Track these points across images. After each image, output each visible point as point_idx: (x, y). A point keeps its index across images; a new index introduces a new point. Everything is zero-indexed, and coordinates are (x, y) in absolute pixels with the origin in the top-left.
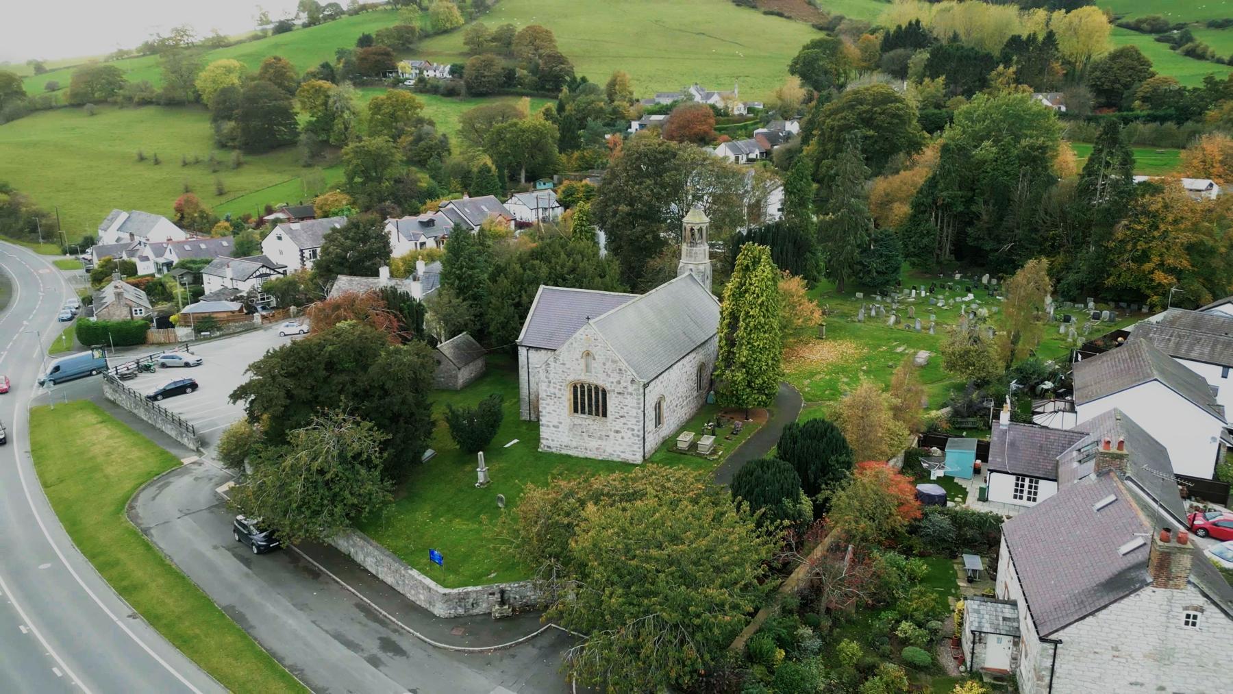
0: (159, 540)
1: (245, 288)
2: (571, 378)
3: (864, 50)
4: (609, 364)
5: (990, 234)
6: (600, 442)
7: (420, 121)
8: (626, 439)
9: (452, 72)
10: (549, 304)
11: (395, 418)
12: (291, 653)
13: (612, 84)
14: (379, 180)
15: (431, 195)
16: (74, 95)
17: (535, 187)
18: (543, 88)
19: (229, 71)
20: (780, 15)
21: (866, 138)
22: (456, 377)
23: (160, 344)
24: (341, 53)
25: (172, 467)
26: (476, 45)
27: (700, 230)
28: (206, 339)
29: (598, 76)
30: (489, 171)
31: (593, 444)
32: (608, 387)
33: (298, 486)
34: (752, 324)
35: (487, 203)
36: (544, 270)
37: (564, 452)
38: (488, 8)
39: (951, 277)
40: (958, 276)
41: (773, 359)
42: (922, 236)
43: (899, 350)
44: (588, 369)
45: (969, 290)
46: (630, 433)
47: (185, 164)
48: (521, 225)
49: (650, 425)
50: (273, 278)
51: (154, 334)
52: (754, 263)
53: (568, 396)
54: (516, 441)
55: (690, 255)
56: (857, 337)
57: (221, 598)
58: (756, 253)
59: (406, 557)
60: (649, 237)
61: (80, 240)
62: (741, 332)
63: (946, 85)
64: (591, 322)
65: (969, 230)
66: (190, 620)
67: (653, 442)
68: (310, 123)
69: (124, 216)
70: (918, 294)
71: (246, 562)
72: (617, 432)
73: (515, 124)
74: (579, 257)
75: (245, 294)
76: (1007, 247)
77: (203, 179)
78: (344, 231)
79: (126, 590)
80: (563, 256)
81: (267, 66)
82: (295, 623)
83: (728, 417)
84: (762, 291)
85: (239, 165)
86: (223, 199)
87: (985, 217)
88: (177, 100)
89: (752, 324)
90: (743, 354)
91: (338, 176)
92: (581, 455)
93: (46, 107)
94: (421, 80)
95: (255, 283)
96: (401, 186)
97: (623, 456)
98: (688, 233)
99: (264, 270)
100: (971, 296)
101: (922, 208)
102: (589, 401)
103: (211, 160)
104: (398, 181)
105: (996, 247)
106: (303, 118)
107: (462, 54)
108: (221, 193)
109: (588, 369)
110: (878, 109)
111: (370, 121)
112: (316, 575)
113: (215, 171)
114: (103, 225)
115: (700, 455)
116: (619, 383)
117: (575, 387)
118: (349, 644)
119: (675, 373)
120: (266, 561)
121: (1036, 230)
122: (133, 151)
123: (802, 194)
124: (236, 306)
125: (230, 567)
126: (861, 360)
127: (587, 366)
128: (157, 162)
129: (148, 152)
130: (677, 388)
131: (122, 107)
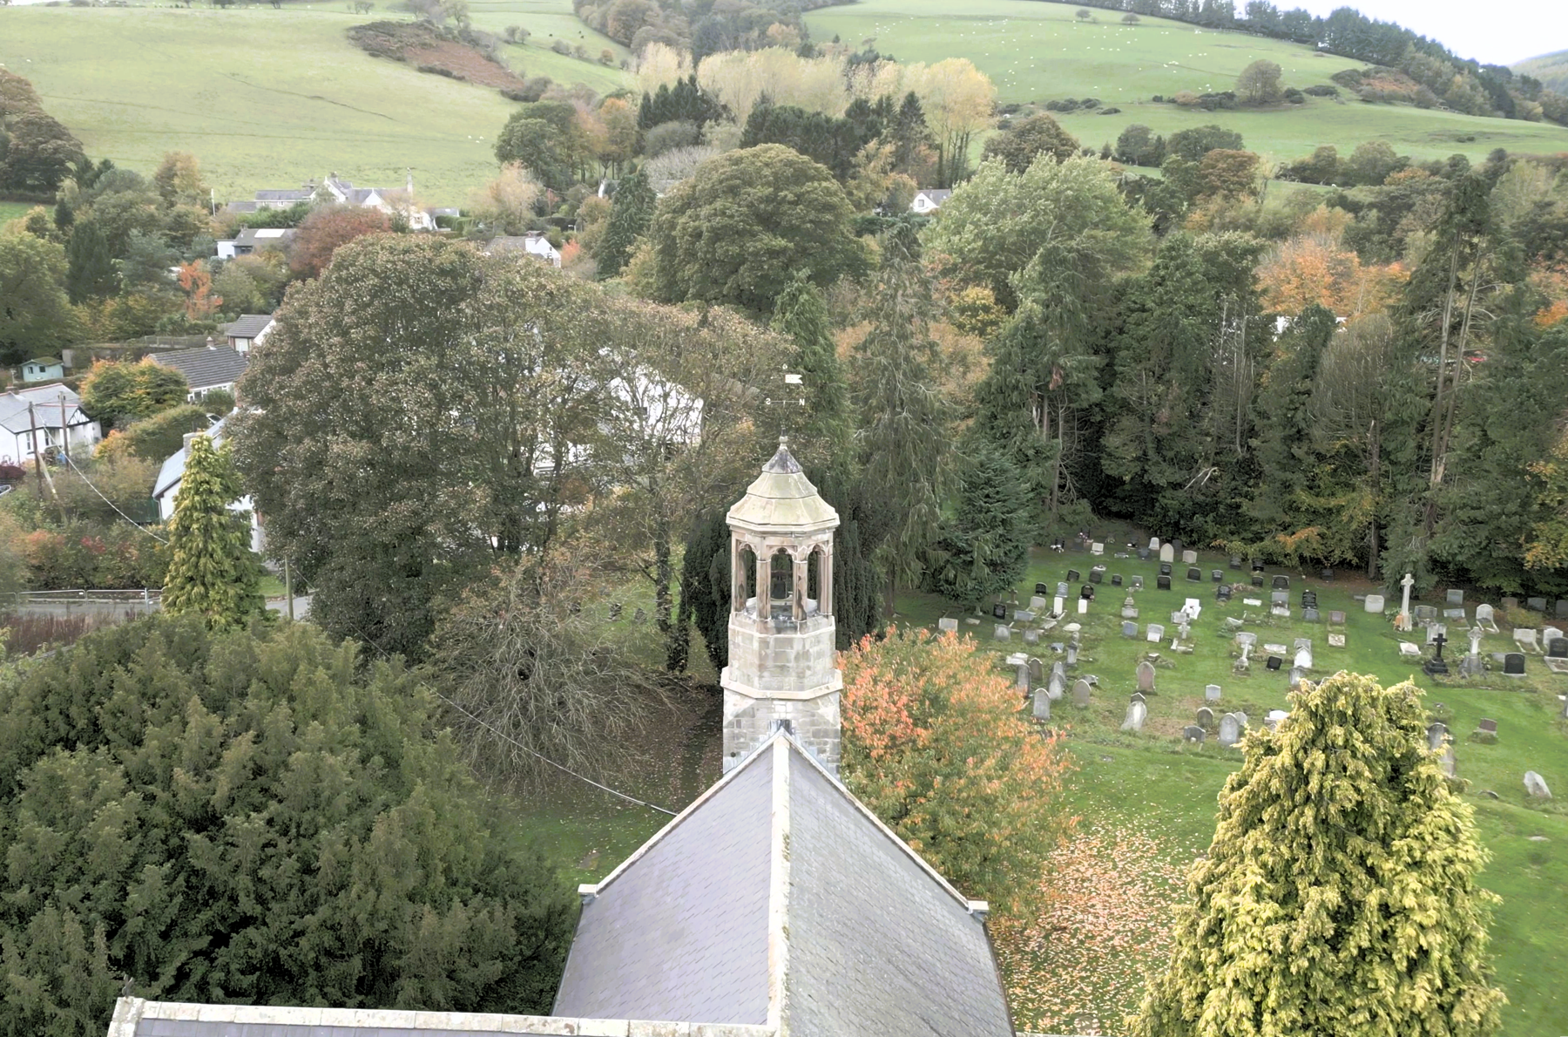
3: (613, 124)
5: (1158, 450)
40: (1098, 548)
45: (1164, 585)
100: (1192, 607)
101: (1015, 397)
105: (1177, 478)
121: (1300, 436)
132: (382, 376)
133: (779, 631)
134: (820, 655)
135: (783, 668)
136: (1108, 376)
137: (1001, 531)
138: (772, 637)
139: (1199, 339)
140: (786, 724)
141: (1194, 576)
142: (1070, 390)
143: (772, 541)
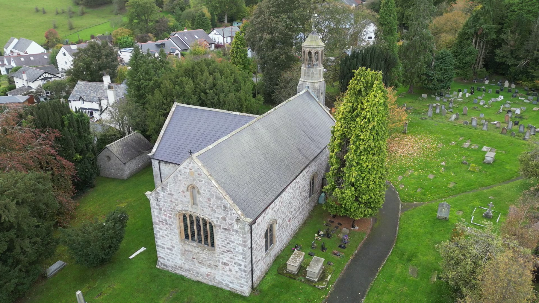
1: (34, 86)
2: (179, 208)
4: (213, 200)
5: (512, 54)
6: (209, 270)
8: (234, 272)
10: (183, 118)
14: (147, 21)
15: (174, 29)
17: (232, 25)
22: (123, 170)
27: (317, 53)
30: (204, 16)
31: (204, 270)
32: (215, 222)
34: (362, 148)
35: (198, 35)
36: (189, 86)
37: (179, 272)
39: (483, 82)
40: (487, 82)
41: (380, 178)
42: (466, 55)
43: (466, 145)
44: (194, 202)
45: (498, 92)
46: (237, 268)
47: (57, 13)
48: (218, 46)
49: (259, 253)
50: (53, 79)
52: (366, 88)
53: (177, 225)
54: (143, 249)
55: (307, 75)
56: (431, 132)
58: (369, 78)
60: (283, 57)
62: (351, 155)
64: (194, 155)
65: (498, 51)
69: (16, 41)
70: (464, 95)
72: (225, 264)
74: (218, 75)
75: (34, 90)
76: (522, 63)
77: (63, 20)
78: (85, 51)
80: (206, 74)
83: (336, 222)
84: (373, 116)
85: (83, 13)
86: (72, 31)
87: (512, 43)
89: (362, 148)
90: (352, 175)
91: (125, 19)
92: (194, 278)
96: (158, 25)
97: (231, 285)
98: (306, 55)
99: (46, 75)
100: (501, 98)
101: (466, 36)
102: (199, 231)
103: (70, 11)
104: (157, 22)
105: (515, 63)
109: (194, 202)
113: (71, 17)
114: (6, 46)
115: (309, 281)
116: (224, 219)
117: (184, 216)
122: (33, 6)
123: (390, 25)
126: (440, 155)
127: (193, 198)
128: (44, 13)
129: (40, 7)
130: (289, 208)
132: (276, 19)
133: (308, 68)
134: (316, 74)
135: (308, 76)
136: (499, 31)
137: (443, 71)
138: (307, 69)
139: (529, 21)
140: (308, 87)
141: (510, 91)
142: (486, 34)
143: (308, 49)
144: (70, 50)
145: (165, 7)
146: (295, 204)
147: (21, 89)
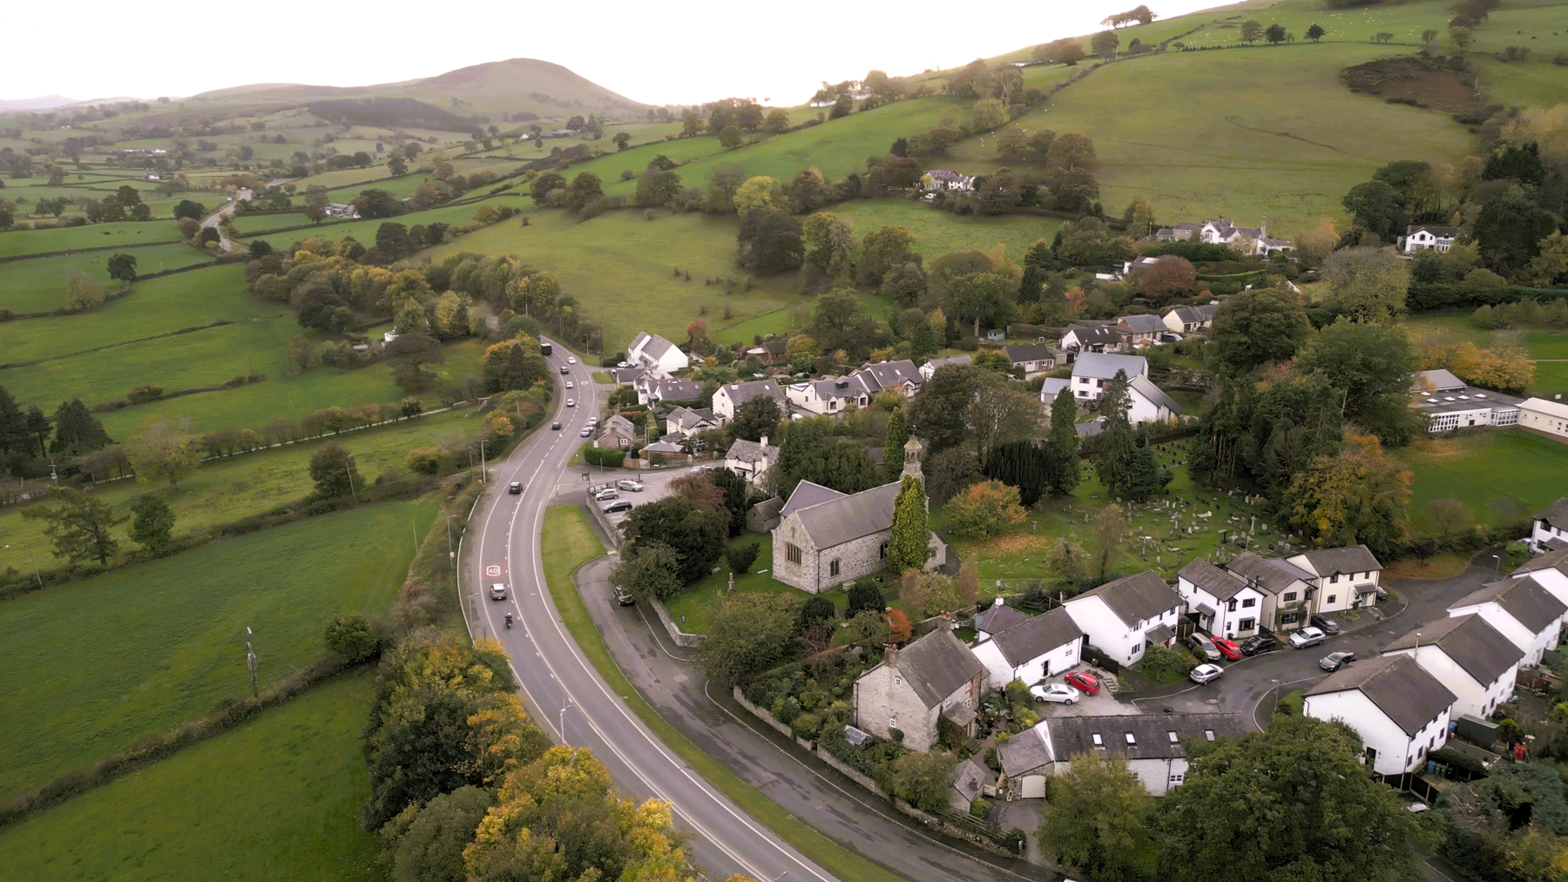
0: (583, 592)
1: (689, 433)
7: (907, 258)
9: (976, 184)
11: (692, 548)
12: (613, 647)
13: (1132, 210)
16: (639, 197)
18: (1062, 208)
19: (762, 187)
20: (1411, 103)
21: (1240, 344)
23: (630, 469)
24: (872, 162)
25: (602, 554)
26: (1011, 155)
28: (657, 469)
29: (1115, 199)
33: (635, 575)
36: (821, 465)
38: (1044, 98)
47: (709, 283)
51: (628, 461)
57: (597, 621)
59: (672, 617)
61: (614, 356)
63: (1482, 249)
66: (584, 627)
67: (827, 582)
68: (813, 253)
69: (648, 338)
71: (614, 608)
73: (971, 279)
77: (715, 298)
79: (562, 611)
81: (799, 180)
82: (622, 639)
85: (749, 288)
88: (717, 210)
93: (615, 206)
94: (940, 196)
95: (695, 430)
102: (794, 555)
106: (810, 247)
107: (996, 161)
108: (728, 317)
110: (1255, 318)
111: (865, 253)
112: (639, 619)
113: (730, 293)
118: (637, 649)
119: (853, 546)
120: (623, 610)
122: (673, 263)
124: (678, 448)
125: (607, 608)
128: (688, 279)
131: (675, 212)
144: (732, 394)
145: (883, 288)
146: (863, 555)
147: (674, 435)
